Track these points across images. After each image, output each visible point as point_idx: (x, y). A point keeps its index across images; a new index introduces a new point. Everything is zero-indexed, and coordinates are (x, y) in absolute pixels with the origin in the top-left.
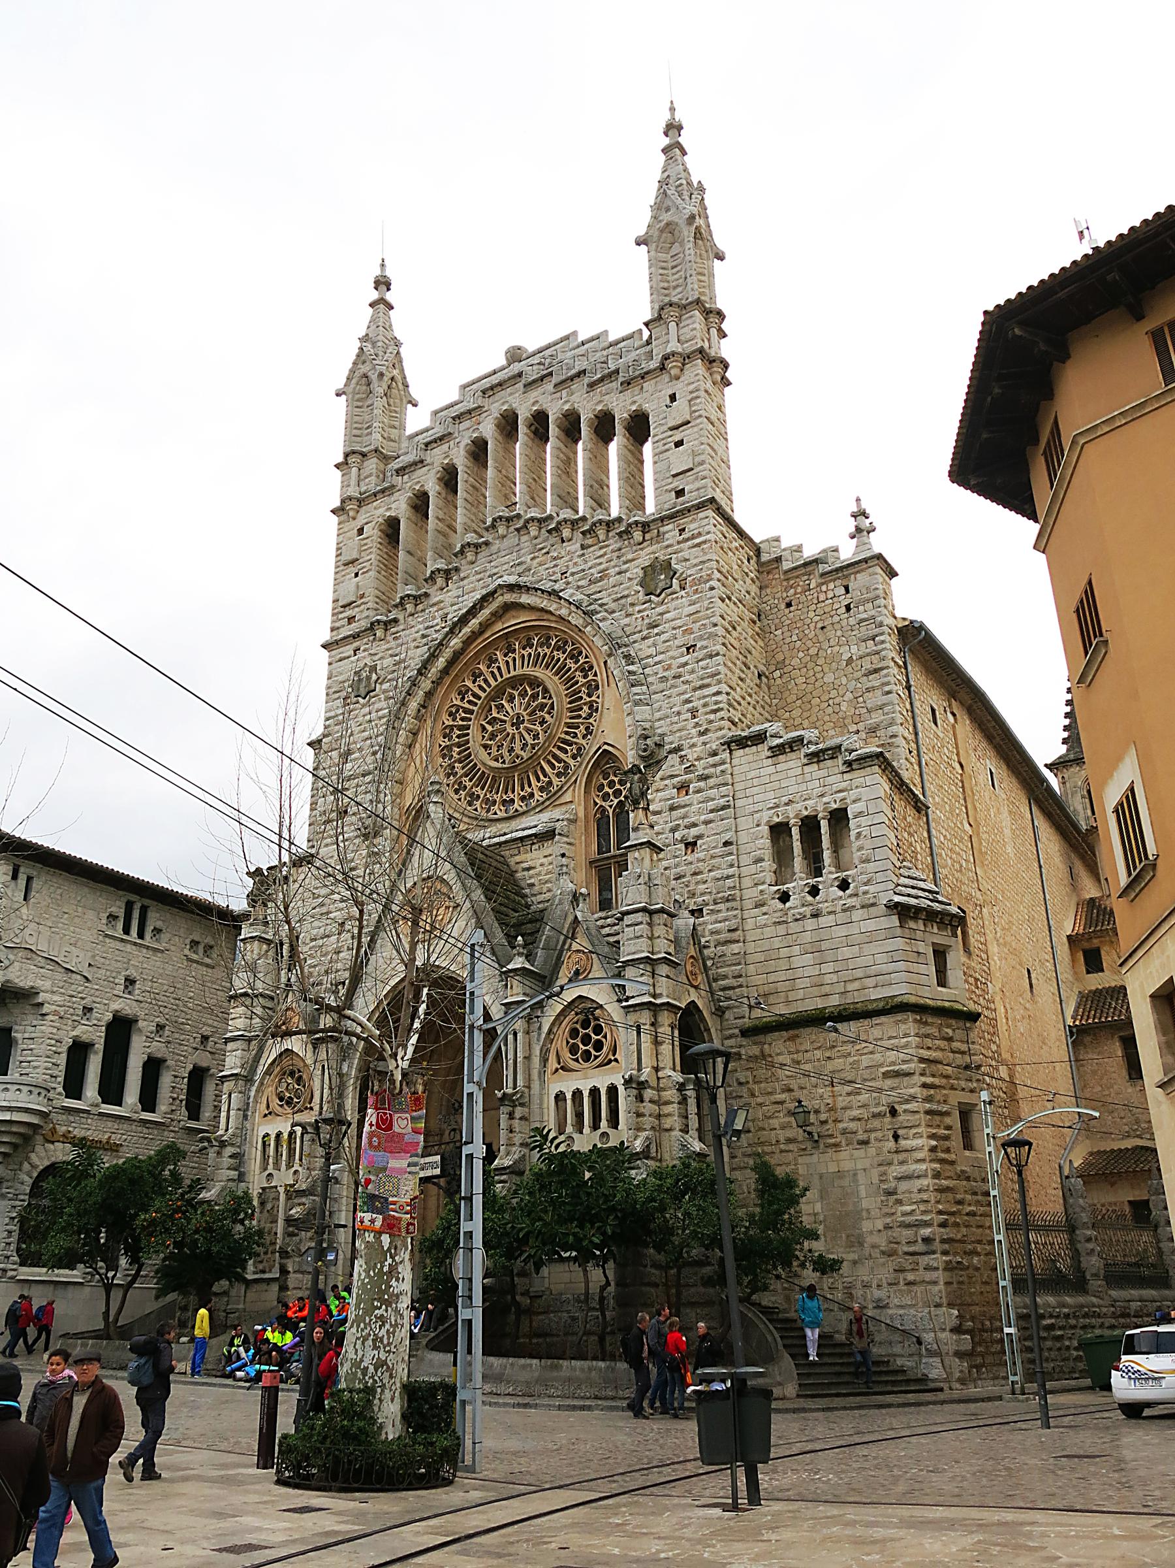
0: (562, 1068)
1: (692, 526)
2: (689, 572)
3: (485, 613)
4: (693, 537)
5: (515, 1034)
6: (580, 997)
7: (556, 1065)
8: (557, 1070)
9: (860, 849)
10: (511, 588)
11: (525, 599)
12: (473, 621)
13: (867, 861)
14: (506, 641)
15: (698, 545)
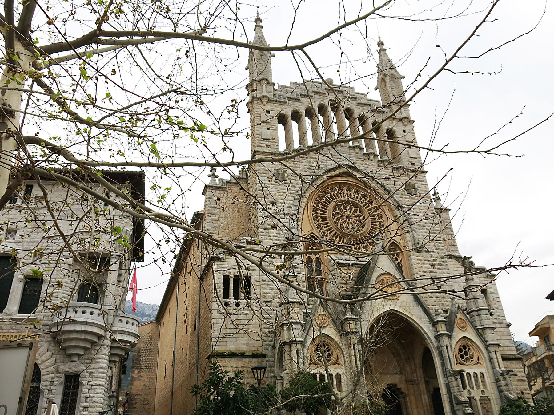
0: (459, 363)
1: (420, 177)
2: (422, 192)
3: (338, 172)
4: (421, 181)
5: (447, 347)
6: (465, 337)
7: (456, 362)
8: (457, 364)
9: (495, 304)
10: (350, 167)
11: (355, 173)
12: (333, 172)
13: (497, 308)
14: (341, 185)
15: (423, 184)
